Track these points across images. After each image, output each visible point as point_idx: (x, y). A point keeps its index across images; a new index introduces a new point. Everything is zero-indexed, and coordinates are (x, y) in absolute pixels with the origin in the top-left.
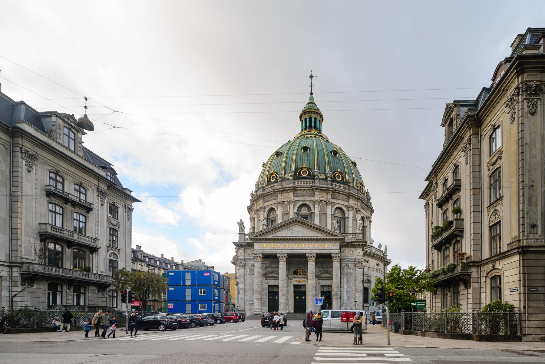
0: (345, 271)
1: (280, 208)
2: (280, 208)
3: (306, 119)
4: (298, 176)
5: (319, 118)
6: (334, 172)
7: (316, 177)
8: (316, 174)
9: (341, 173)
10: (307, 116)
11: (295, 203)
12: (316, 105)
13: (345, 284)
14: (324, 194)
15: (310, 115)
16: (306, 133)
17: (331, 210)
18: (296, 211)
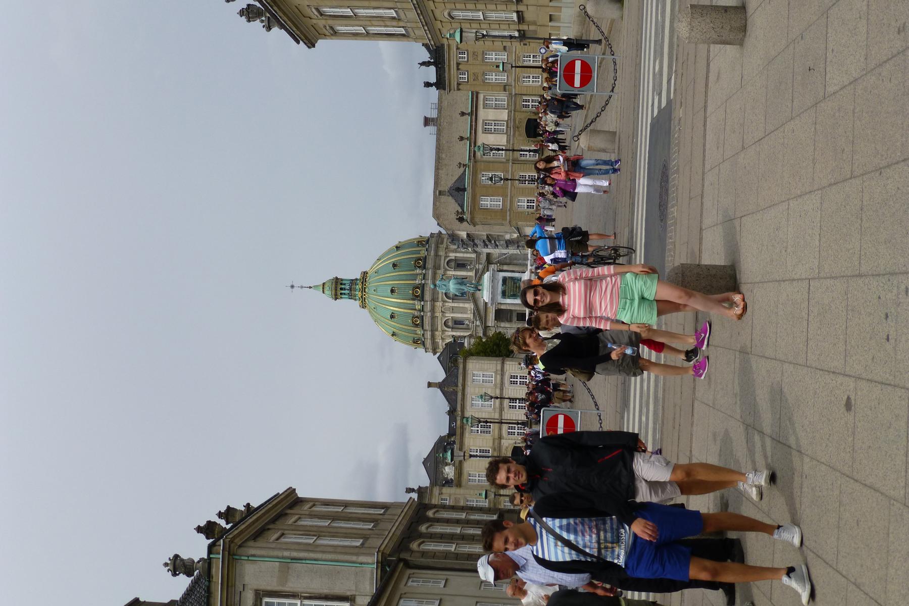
0: (508, 261)
1: (447, 315)
2: (447, 315)
3: (341, 294)
4: (421, 298)
5: (340, 282)
6: (415, 267)
7: (423, 282)
8: (420, 282)
9: (416, 261)
10: (339, 292)
11: (444, 301)
12: (324, 283)
13: (518, 262)
14: (437, 275)
15: (338, 289)
16: (360, 293)
17: (449, 270)
18: (451, 301)
